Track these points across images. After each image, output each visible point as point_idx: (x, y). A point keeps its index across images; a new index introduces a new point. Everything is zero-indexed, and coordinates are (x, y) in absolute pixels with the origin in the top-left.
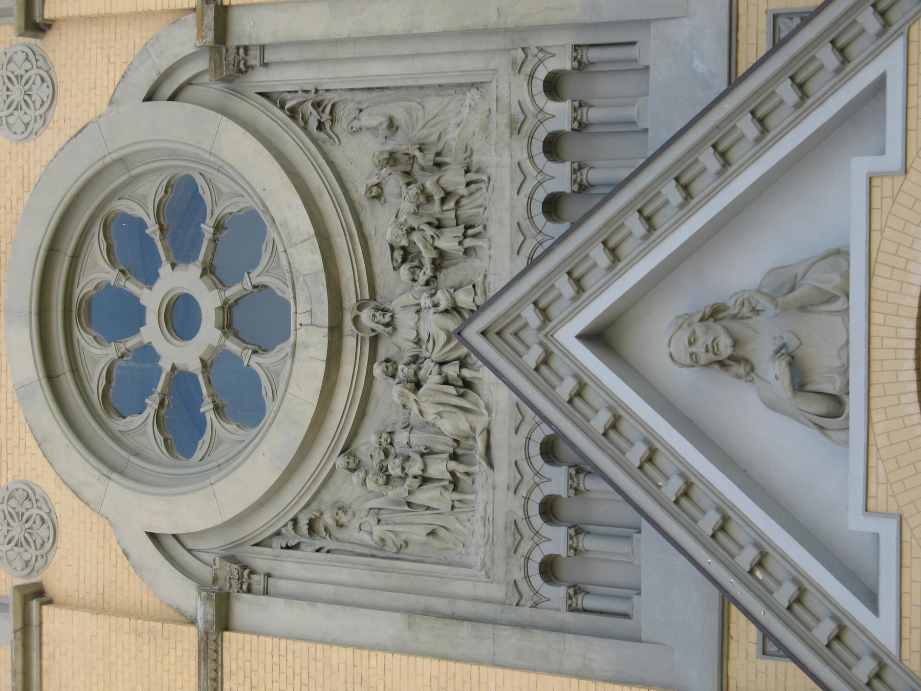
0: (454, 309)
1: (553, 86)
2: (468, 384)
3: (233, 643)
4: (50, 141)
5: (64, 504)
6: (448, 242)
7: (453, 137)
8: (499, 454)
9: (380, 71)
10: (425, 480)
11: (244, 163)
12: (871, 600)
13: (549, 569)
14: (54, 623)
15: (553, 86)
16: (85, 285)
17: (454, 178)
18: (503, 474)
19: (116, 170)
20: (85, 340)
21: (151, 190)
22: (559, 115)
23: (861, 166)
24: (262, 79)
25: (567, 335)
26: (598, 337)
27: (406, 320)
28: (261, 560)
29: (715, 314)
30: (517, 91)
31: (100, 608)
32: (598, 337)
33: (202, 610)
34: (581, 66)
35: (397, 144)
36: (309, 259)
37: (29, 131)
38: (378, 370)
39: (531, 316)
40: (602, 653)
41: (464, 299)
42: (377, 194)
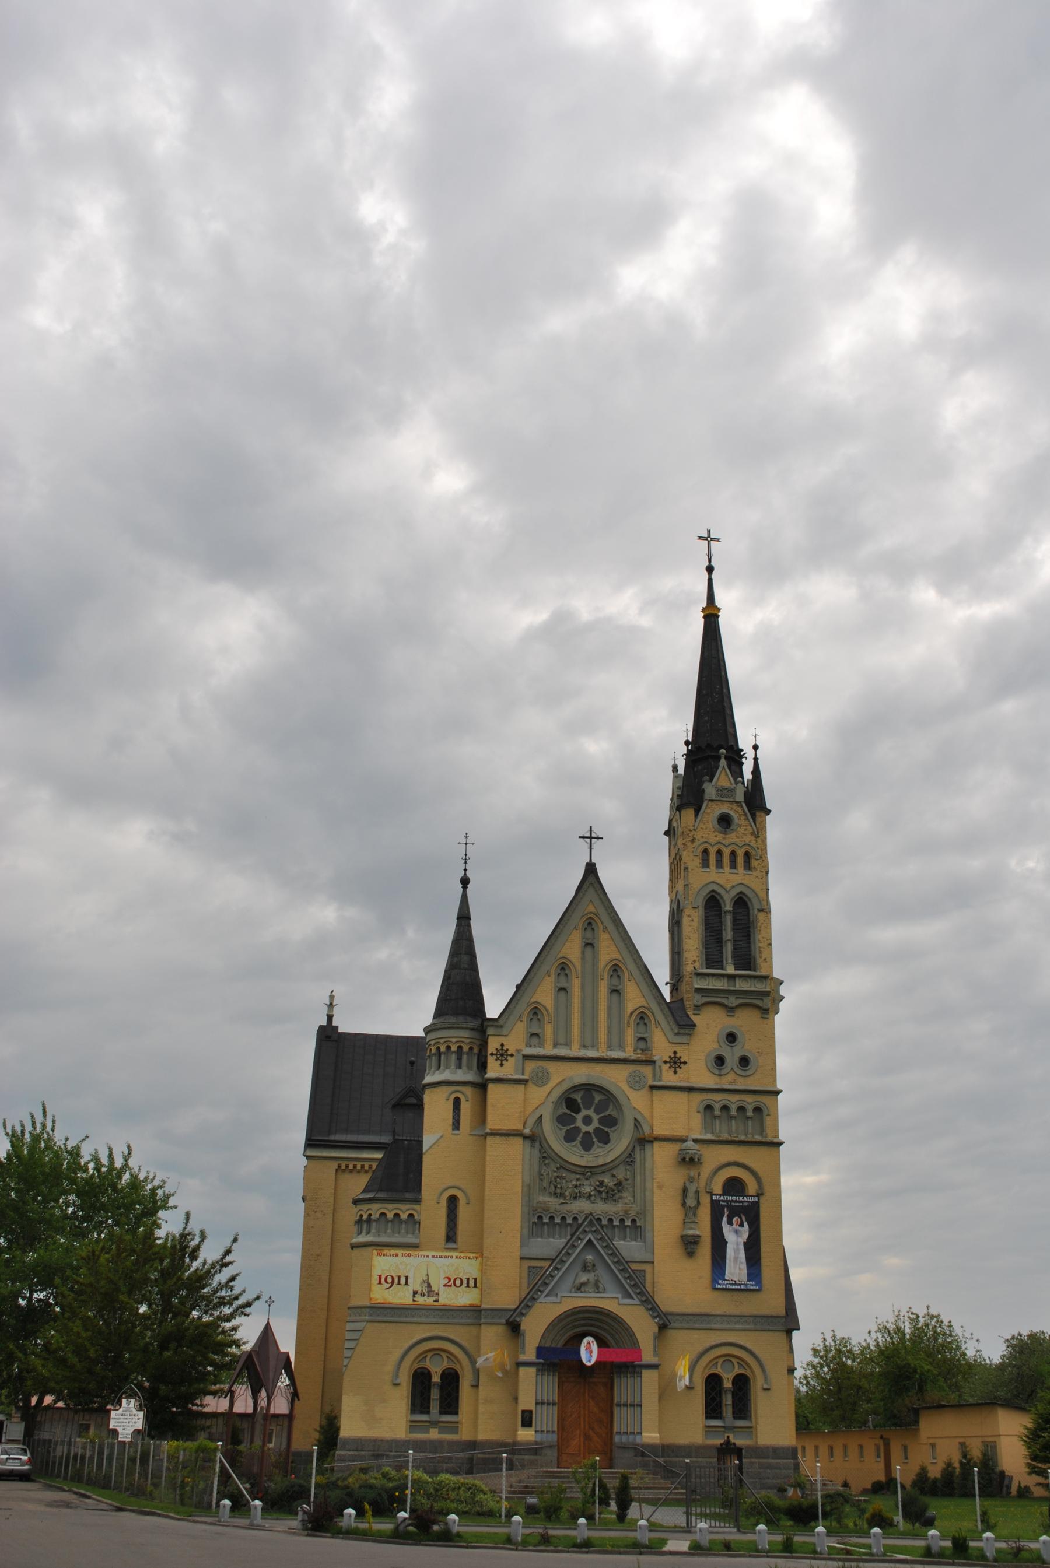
0: (590, 1195)
1: (634, 1221)
2: (575, 1198)
3: (520, 1140)
4: (625, 1088)
5: (547, 1089)
6: (604, 1195)
7: (625, 1194)
8: (562, 1207)
9: (638, 1178)
10: (556, 1187)
11: (621, 1142)
12: (547, 1296)
13: (540, 1218)
14: (521, 1087)
15: (634, 1221)
16: (595, 1094)
17: (617, 1196)
18: (558, 1207)
19: (618, 1106)
20: (581, 1093)
21: (614, 1113)
22: (628, 1223)
23: (620, 1296)
24: (638, 1149)
25: (590, 1236)
26: (590, 1240)
27: (588, 1182)
28: (537, 1144)
29: (594, 1265)
30: (633, 1213)
31: (525, 1100)
32: (590, 1240)
33: (527, 1131)
34: (637, 1227)
35: (624, 1183)
36: (601, 1162)
37: (628, 1082)
38: (578, 1176)
39: (594, 1229)
40: (526, 1231)
41: (593, 1198)
42: (613, 1176)
